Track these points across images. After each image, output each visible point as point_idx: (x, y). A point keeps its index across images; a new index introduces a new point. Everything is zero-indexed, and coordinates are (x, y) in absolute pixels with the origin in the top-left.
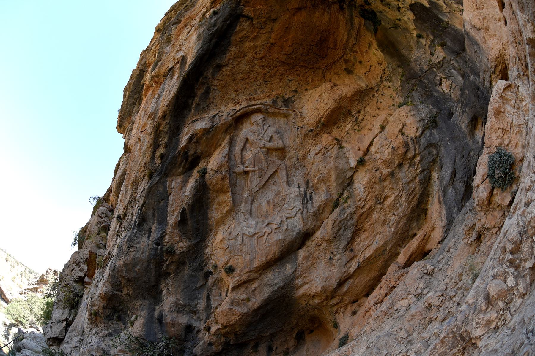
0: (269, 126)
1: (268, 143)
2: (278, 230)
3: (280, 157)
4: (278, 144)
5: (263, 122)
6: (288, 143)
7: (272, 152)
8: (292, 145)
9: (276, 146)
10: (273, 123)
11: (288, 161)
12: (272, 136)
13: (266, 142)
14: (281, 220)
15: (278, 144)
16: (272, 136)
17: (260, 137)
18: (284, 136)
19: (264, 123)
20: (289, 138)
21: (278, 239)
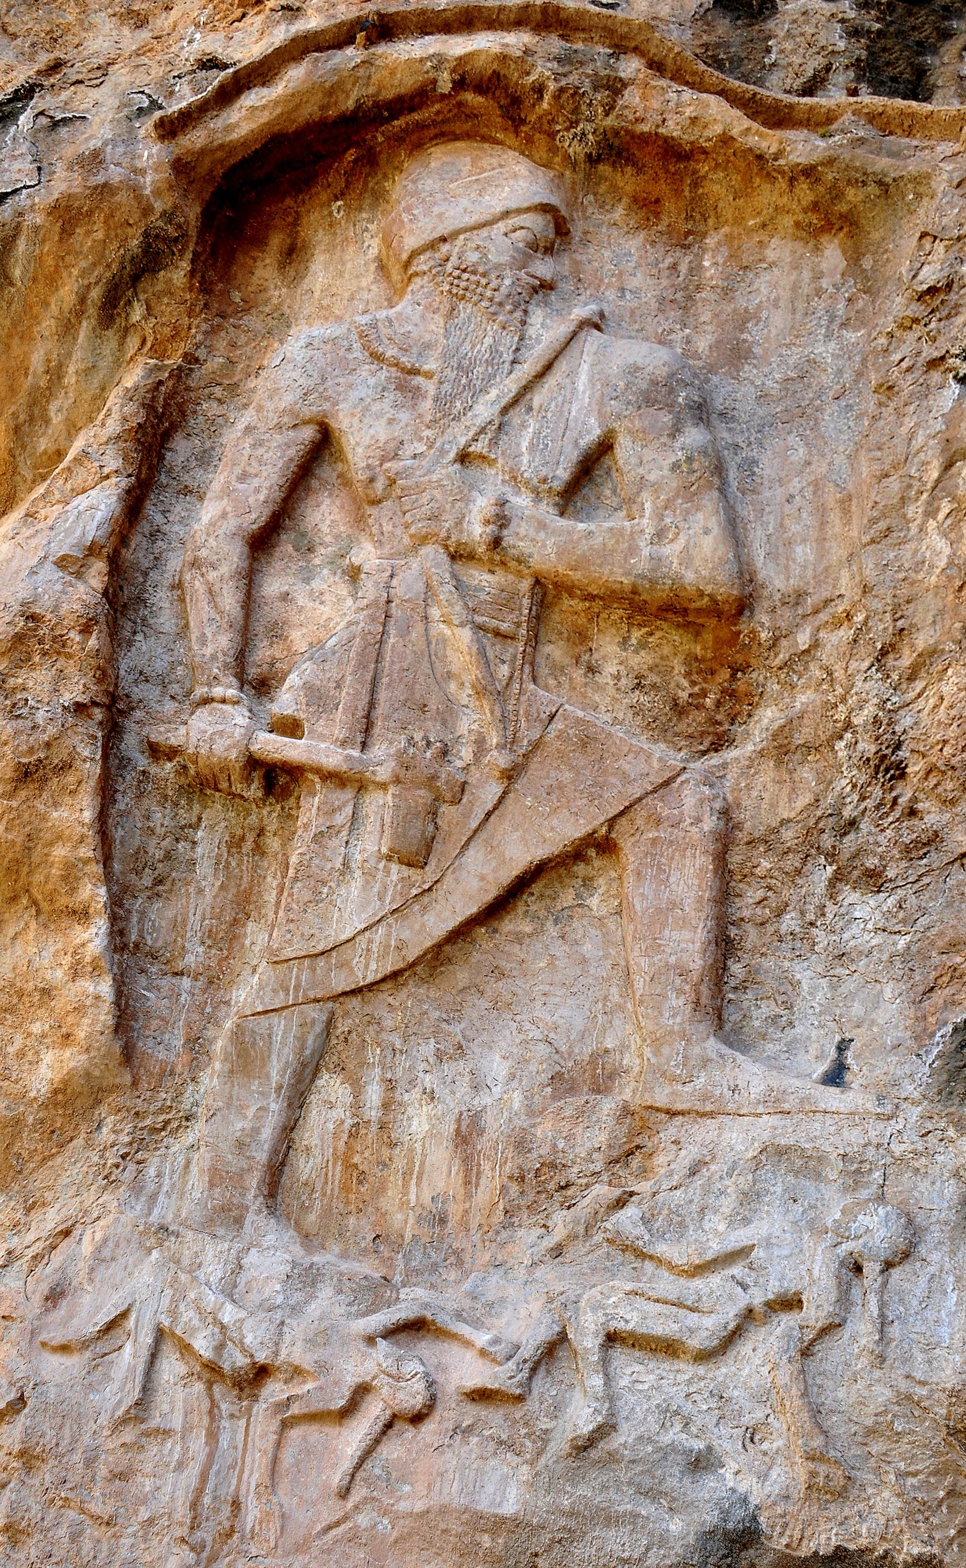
0: (596, 324)
1: (547, 510)
2: (494, 1417)
3: (679, 710)
4: (671, 551)
5: (522, 261)
6: (803, 553)
7: (581, 637)
8: (846, 584)
9: (641, 563)
10: (650, 297)
11: (767, 773)
12: (605, 447)
13: (522, 501)
14: (544, 1332)
15: (671, 551)
16: (605, 447)
17: (459, 436)
18: (768, 467)
19: (544, 268)
20: (831, 497)
21: (483, 1505)
